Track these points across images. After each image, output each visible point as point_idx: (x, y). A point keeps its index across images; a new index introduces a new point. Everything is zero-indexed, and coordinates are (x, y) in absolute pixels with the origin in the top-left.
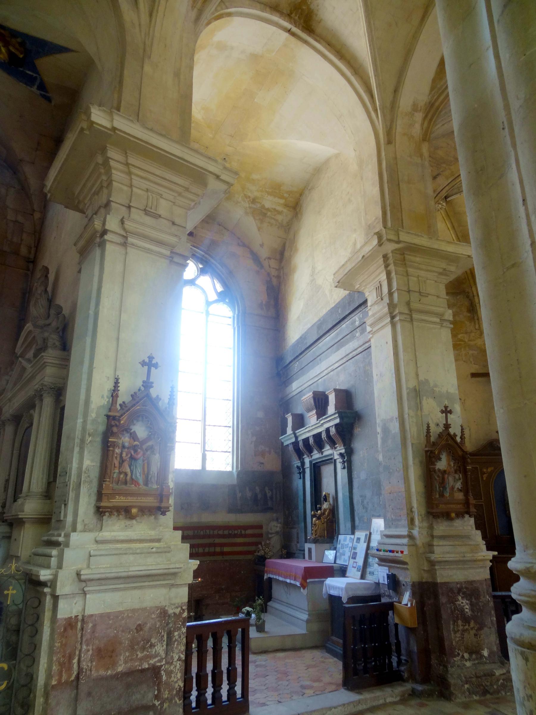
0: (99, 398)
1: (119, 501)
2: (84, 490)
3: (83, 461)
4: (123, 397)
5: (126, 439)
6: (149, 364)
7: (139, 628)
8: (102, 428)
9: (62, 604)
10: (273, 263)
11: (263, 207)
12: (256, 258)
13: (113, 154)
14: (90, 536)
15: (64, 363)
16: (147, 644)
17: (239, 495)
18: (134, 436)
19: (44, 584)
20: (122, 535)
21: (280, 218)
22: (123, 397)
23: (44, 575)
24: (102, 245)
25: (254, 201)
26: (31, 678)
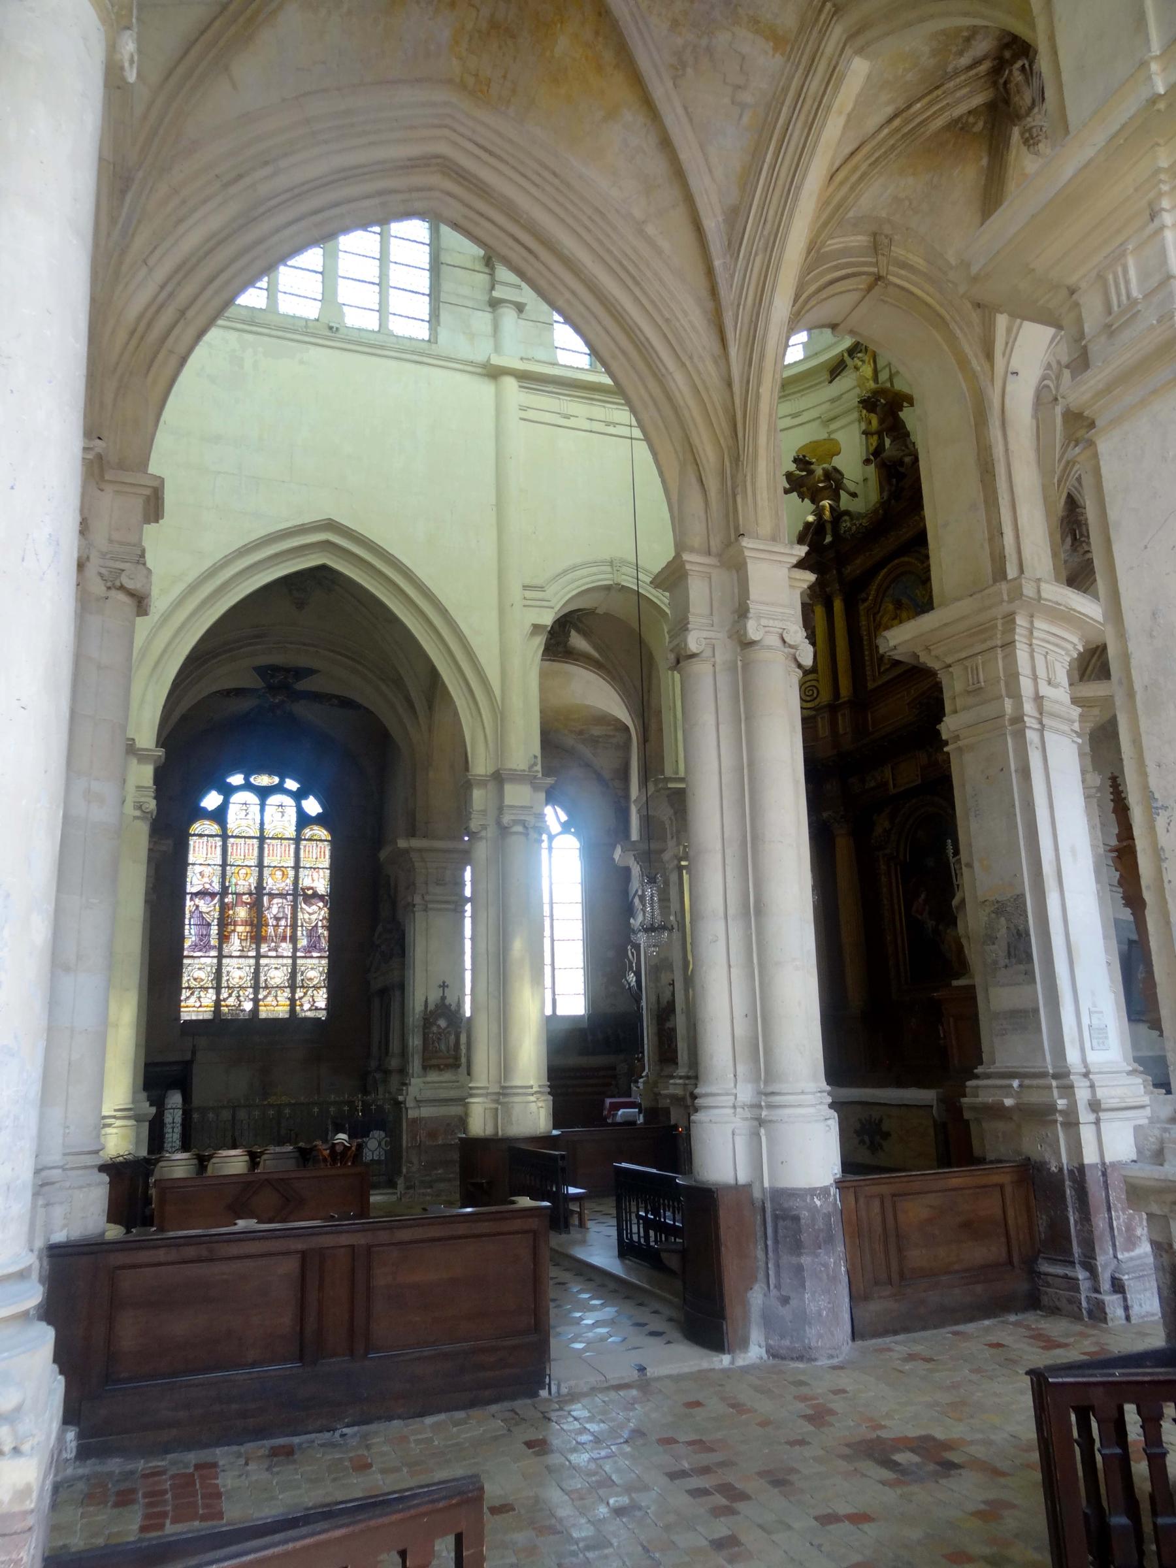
0: (419, 1007)
2: (416, 1056)
3: (415, 1042)
4: (431, 1007)
5: (435, 1029)
7: (448, 1125)
8: (422, 1023)
12: (599, 777)
13: (415, 856)
14: (420, 1080)
15: (403, 967)
17: (590, 1038)
18: (439, 1026)
19: (401, 1103)
23: (401, 1098)
24: (414, 912)
25: (581, 733)
26: (401, 1145)
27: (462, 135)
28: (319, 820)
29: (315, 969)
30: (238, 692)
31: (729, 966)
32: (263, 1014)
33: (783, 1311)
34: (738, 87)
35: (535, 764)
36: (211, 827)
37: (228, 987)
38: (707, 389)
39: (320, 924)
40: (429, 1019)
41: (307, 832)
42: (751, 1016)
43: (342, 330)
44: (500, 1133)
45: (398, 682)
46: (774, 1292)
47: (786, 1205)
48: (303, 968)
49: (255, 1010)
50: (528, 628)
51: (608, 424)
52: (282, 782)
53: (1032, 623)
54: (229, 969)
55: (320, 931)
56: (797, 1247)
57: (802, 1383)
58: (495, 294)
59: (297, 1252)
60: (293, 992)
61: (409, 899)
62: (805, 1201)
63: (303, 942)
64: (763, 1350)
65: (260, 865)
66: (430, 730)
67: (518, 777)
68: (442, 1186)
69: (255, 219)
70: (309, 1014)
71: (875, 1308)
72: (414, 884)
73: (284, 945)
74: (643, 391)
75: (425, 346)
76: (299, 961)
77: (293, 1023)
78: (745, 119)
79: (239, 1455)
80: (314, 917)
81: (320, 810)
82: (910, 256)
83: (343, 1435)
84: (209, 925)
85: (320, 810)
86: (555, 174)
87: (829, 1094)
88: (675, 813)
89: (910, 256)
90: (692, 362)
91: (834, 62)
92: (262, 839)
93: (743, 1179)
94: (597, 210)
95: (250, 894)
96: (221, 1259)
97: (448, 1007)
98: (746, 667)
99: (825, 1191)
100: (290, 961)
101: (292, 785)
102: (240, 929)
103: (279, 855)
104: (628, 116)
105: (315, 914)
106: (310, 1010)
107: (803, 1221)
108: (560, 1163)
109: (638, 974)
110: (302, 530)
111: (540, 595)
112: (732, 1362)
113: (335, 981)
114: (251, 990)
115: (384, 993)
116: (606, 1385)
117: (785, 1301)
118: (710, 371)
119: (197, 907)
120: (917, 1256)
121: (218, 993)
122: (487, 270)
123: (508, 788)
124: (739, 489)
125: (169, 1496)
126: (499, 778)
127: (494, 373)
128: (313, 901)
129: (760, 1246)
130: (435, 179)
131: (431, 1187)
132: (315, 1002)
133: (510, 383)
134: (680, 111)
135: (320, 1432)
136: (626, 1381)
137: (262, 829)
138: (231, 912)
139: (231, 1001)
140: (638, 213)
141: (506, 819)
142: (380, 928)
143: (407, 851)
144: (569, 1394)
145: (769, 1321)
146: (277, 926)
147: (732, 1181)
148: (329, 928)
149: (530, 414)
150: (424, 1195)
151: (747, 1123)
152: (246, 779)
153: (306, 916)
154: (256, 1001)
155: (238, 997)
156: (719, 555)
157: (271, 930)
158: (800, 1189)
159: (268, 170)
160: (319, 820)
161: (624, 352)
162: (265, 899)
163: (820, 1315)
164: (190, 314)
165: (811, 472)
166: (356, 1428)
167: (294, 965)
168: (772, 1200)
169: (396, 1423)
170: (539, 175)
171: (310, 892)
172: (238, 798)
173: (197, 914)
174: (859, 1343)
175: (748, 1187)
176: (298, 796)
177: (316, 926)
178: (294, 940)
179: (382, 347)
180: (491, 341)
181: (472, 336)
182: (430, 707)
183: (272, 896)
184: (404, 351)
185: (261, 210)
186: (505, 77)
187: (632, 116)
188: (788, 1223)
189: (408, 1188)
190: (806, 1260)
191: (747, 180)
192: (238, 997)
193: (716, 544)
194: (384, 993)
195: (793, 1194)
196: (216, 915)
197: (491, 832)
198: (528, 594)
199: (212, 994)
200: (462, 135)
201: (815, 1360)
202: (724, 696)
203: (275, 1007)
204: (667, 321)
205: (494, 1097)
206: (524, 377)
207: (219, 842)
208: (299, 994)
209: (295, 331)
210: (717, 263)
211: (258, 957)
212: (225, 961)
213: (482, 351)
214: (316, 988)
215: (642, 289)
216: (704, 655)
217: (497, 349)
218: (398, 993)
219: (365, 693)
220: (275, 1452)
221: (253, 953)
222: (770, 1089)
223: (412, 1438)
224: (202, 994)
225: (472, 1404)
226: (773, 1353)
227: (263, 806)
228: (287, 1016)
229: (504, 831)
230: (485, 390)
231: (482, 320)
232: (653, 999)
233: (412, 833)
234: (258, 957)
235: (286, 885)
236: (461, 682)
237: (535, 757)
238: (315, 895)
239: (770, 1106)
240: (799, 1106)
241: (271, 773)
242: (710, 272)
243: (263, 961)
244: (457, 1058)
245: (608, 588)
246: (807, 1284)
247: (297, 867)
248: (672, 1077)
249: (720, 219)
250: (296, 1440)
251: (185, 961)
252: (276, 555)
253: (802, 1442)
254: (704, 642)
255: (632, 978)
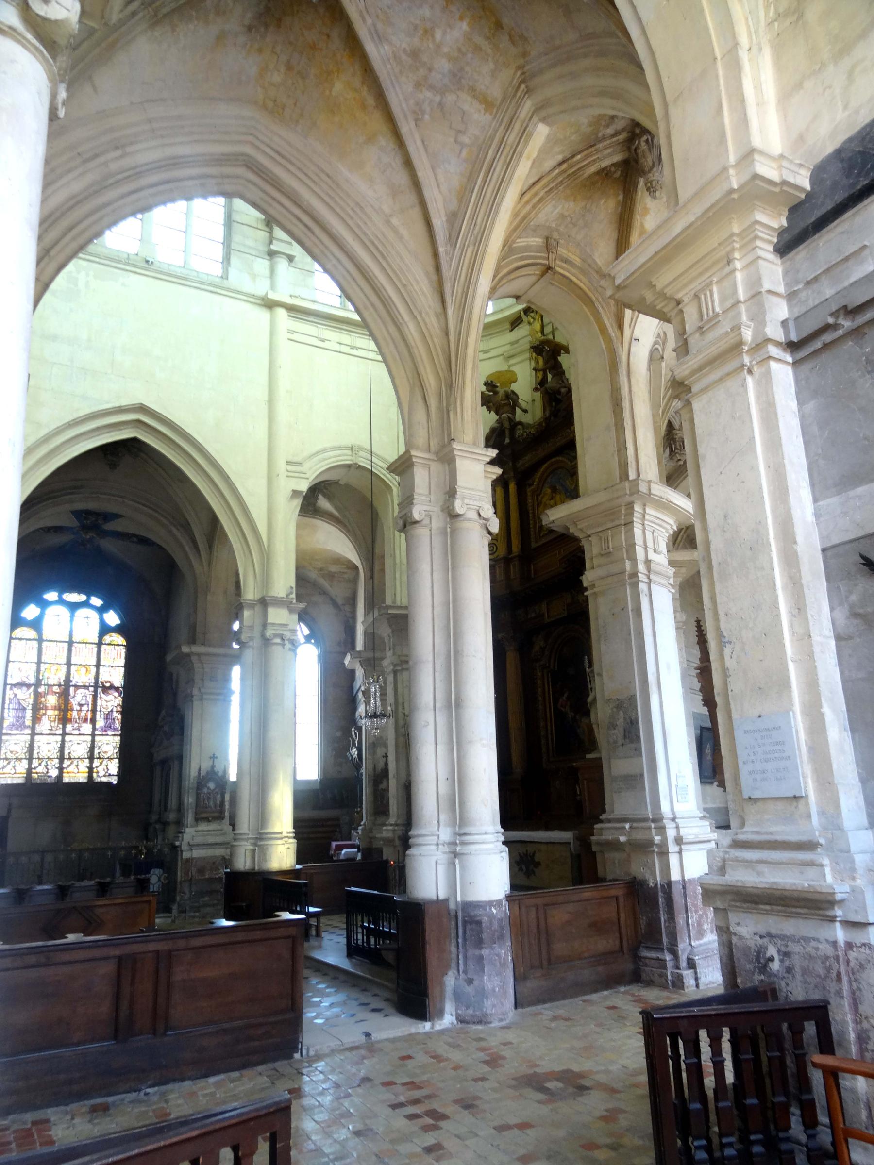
0: (194, 773)
1: (204, 815)
3: (190, 800)
4: (203, 773)
5: (205, 790)
6: (213, 757)
7: (214, 863)
8: (196, 786)
9: (184, 853)
10: (347, 608)
11: (330, 572)
13: (194, 659)
15: (181, 743)
16: (217, 869)
18: (209, 788)
19: (177, 847)
20: (206, 828)
21: (346, 576)
22: (203, 773)
23: (177, 843)
25: (321, 569)
26: (176, 880)
27: (263, 142)
28: (118, 630)
29: (110, 744)
30: (58, 529)
31: (436, 744)
32: (66, 779)
33: (470, 990)
34: (460, 131)
35: (291, 593)
36: (31, 633)
37: (39, 758)
38: (431, 336)
39: (115, 709)
40: (201, 783)
41: (107, 639)
42: (451, 779)
43: (155, 263)
44: (257, 868)
45: (186, 527)
46: (462, 975)
47: (472, 914)
48: (100, 744)
49: (60, 777)
50: (290, 493)
51: (352, 348)
52: (89, 598)
53: (644, 510)
54: (39, 744)
55: (115, 714)
56: (479, 943)
57: (481, 1039)
58: (272, 247)
59: (114, 957)
60: (91, 762)
61: (189, 691)
62: (485, 909)
63: (100, 723)
64: (454, 1018)
65: (69, 664)
66: (209, 564)
67: (279, 603)
68: (208, 910)
69: (106, 187)
70: (105, 779)
71: (532, 985)
72: (193, 680)
73: (84, 725)
74: (385, 333)
75: (218, 280)
76: (97, 738)
77: (91, 787)
78: (464, 153)
79: (67, 1113)
80: (109, 704)
81: (119, 622)
82: (570, 254)
83: (146, 1094)
84: (24, 709)
85: (119, 622)
86: (328, 176)
87: (503, 834)
88: (393, 632)
89: (570, 254)
90: (421, 316)
91: (525, 125)
92: (70, 643)
93: (442, 895)
94: (357, 204)
95: (60, 685)
96: (55, 964)
97: (216, 773)
98: (453, 531)
99: (499, 902)
100: (89, 738)
101: (96, 601)
102: (50, 712)
103: (85, 655)
104: (383, 141)
105: (112, 702)
106: (105, 776)
107: (484, 925)
108: (304, 889)
109: (360, 750)
110: (120, 410)
111: (298, 469)
112: (432, 1028)
113: (125, 754)
114: (57, 761)
115: (164, 762)
116: (342, 1048)
117: (470, 982)
118: (433, 323)
119: (16, 695)
120: (560, 948)
121: (30, 763)
122: (267, 229)
123: (271, 611)
124: (452, 407)
125: (13, 1145)
126: (264, 603)
127: (270, 305)
128: (110, 692)
129: (453, 943)
130: (241, 171)
131: (199, 911)
132: (108, 770)
133: (281, 312)
134: (419, 143)
135: (128, 1092)
136: (357, 1044)
137: (71, 636)
138: (43, 699)
139: (41, 769)
140: (386, 209)
141: (269, 633)
142: (163, 712)
143: (188, 655)
144: (316, 1055)
145: (458, 997)
146: (81, 710)
147: (435, 898)
148: (122, 713)
149: (295, 336)
150: (194, 917)
151: (446, 856)
152: (60, 596)
153: (104, 703)
154: (61, 769)
155: (46, 766)
156: (437, 454)
157: (75, 714)
158: (483, 902)
159: (118, 153)
160: (118, 630)
161: (373, 305)
162: (72, 689)
163: (494, 991)
164: (53, 253)
165: (496, 393)
166: (156, 1089)
167: (93, 741)
168: (463, 910)
169: (187, 1083)
170: (317, 175)
171: (108, 685)
172: (51, 611)
173: (15, 700)
174: (520, 1010)
175: (446, 901)
176: (101, 610)
177: (112, 711)
178: (93, 721)
179: (186, 279)
180: (268, 281)
181: (254, 277)
182: (211, 547)
183: (77, 687)
184: (202, 283)
185: (111, 181)
186: (295, 104)
187: (385, 141)
188: (474, 926)
189: (183, 911)
190: (485, 952)
191: (463, 195)
192: (46, 766)
193: (434, 444)
194: (164, 762)
195: (477, 905)
196: (31, 701)
197: (257, 642)
198: (290, 468)
199: (25, 764)
200: (263, 142)
201: (491, 1023)
202: (437, 553)
203: (76, 774)
204: (405, 286)
205: (252, 841)
206: (292, 309)
207: (35, 644)
208: (96, 763)
209: (119, 262)
210: (441, 250)
211: (64, 734)
212: (37, 738)
213: (261, 288)
214: (109, 759)
215: (387, 262)
216: (424, 522)
217: (273, 287)
218: (176, 762)
219: (159, 534)
220: (94, 1109)
221: (60, 732)
222: (463, 832)
223: (200, 1093)
224: (17, 763)
225: (243, 1067)
226: (461, 1020)
227: (72, 617)
228: (85, 781)
229: (266, 642)
230: (264, 315)
231: (262, 265)
232: (371, 767)
233: (193, 641)
234: (64, 734)
235: (90, 679)
236: (238, 531)
237: (292, 588)
238: (112, 687)
239: (463, 843)
240: (483, 843)
241: (79, 592)
242: (436, 255)
243: (67, 738)
244: (222, 812)
245: (349, 466)
246: (486, 969)
247: (98, 665)
248: (386, 825)
249: (444, 219)
250: (110, 1099)
251: (4, 738)
252: (98, 429)
253: (483, 1079)
254: (424, 513)
255: (354, 752)
